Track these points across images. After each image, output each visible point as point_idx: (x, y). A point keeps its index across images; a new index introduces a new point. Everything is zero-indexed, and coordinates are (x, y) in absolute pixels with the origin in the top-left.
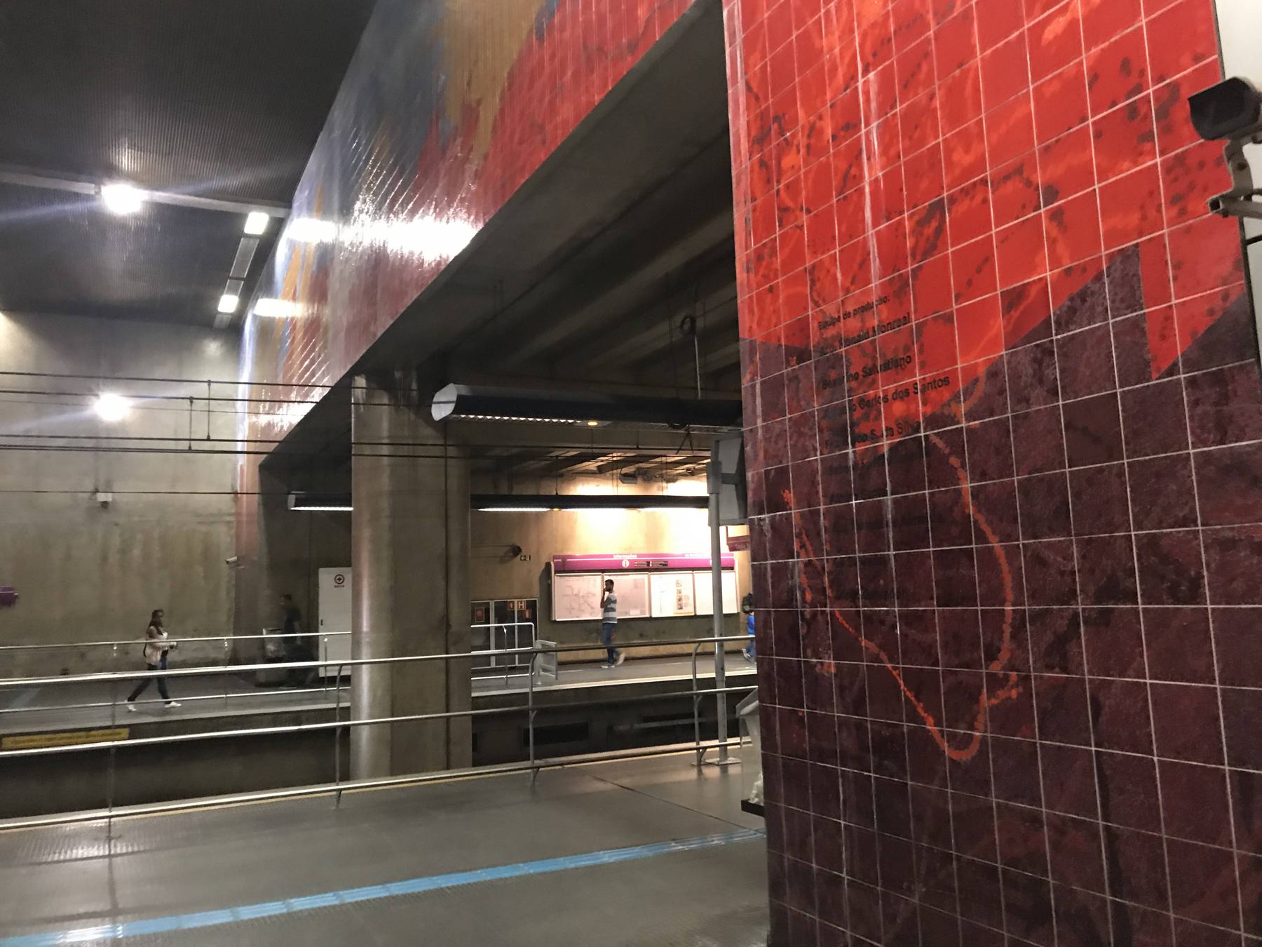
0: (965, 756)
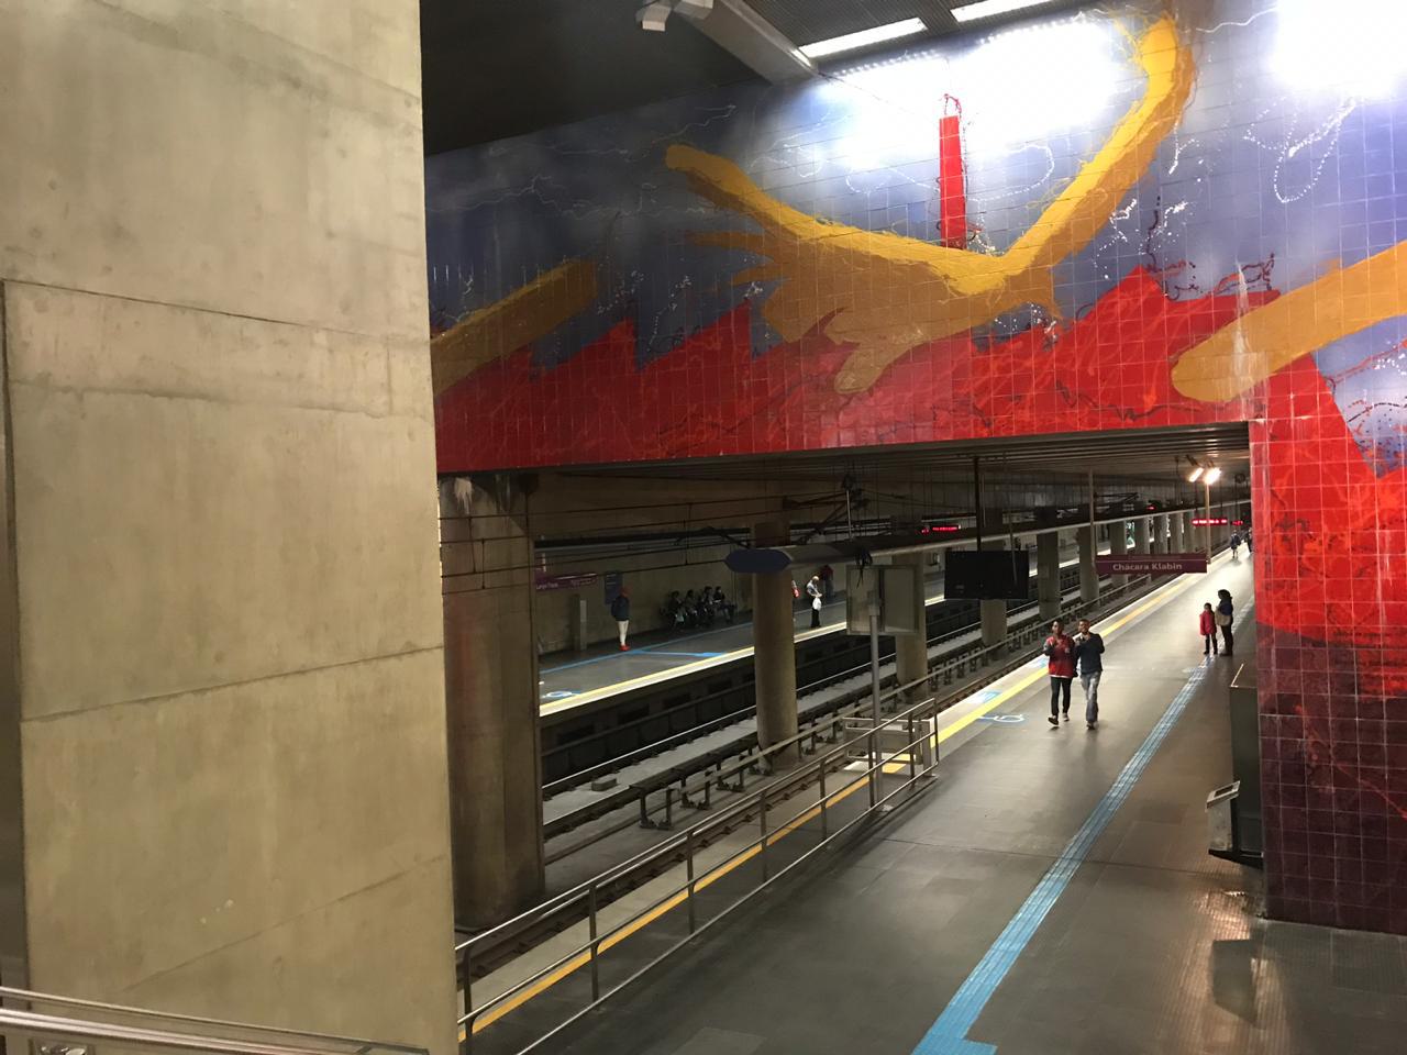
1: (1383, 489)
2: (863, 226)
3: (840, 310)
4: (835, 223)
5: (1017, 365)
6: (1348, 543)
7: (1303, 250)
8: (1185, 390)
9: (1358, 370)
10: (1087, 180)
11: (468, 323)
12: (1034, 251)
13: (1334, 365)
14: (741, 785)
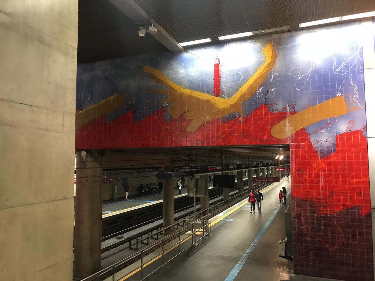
0: (334, 249)
1: (321, 162)
2: (194, 90)
3: (188, 111)
4: (187, 89)
5: (232, 127)
6: (313, 176)
7: (303, 102)
8: (274, 135)
9: (316, 132)
10: (251, 81)
11: (87, 109)
12: (237, 99)
13: (310, 131)
14: (148, 243)
